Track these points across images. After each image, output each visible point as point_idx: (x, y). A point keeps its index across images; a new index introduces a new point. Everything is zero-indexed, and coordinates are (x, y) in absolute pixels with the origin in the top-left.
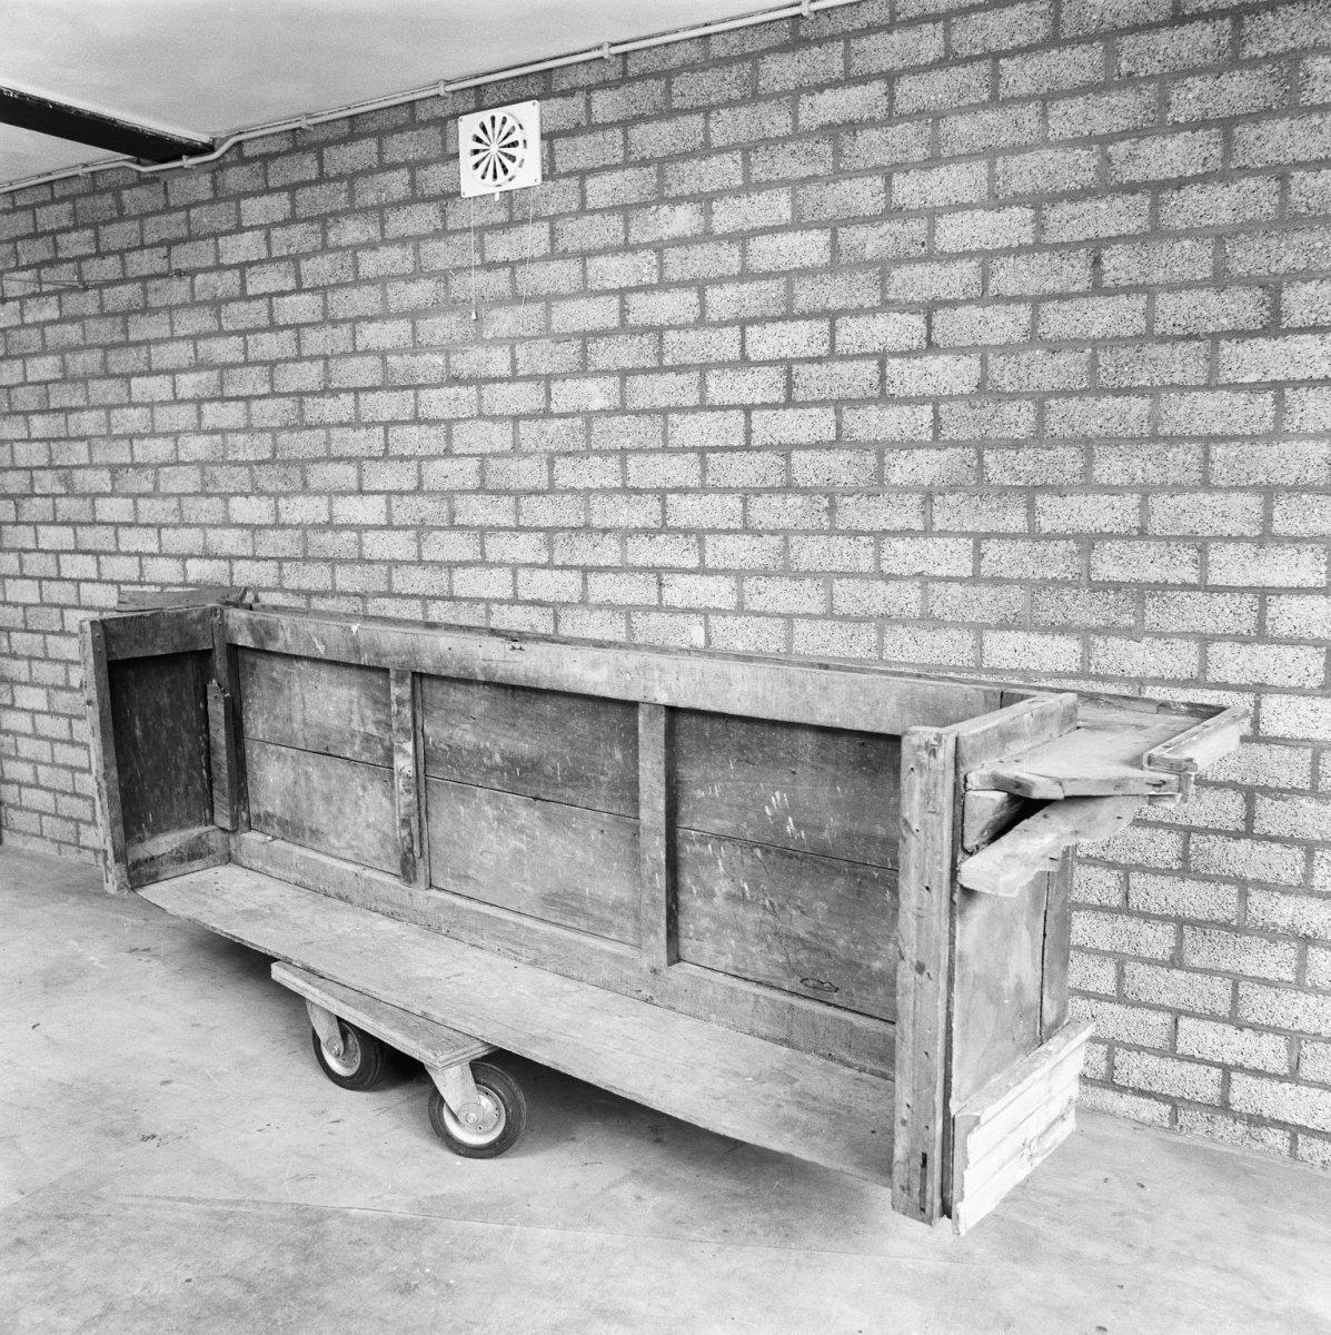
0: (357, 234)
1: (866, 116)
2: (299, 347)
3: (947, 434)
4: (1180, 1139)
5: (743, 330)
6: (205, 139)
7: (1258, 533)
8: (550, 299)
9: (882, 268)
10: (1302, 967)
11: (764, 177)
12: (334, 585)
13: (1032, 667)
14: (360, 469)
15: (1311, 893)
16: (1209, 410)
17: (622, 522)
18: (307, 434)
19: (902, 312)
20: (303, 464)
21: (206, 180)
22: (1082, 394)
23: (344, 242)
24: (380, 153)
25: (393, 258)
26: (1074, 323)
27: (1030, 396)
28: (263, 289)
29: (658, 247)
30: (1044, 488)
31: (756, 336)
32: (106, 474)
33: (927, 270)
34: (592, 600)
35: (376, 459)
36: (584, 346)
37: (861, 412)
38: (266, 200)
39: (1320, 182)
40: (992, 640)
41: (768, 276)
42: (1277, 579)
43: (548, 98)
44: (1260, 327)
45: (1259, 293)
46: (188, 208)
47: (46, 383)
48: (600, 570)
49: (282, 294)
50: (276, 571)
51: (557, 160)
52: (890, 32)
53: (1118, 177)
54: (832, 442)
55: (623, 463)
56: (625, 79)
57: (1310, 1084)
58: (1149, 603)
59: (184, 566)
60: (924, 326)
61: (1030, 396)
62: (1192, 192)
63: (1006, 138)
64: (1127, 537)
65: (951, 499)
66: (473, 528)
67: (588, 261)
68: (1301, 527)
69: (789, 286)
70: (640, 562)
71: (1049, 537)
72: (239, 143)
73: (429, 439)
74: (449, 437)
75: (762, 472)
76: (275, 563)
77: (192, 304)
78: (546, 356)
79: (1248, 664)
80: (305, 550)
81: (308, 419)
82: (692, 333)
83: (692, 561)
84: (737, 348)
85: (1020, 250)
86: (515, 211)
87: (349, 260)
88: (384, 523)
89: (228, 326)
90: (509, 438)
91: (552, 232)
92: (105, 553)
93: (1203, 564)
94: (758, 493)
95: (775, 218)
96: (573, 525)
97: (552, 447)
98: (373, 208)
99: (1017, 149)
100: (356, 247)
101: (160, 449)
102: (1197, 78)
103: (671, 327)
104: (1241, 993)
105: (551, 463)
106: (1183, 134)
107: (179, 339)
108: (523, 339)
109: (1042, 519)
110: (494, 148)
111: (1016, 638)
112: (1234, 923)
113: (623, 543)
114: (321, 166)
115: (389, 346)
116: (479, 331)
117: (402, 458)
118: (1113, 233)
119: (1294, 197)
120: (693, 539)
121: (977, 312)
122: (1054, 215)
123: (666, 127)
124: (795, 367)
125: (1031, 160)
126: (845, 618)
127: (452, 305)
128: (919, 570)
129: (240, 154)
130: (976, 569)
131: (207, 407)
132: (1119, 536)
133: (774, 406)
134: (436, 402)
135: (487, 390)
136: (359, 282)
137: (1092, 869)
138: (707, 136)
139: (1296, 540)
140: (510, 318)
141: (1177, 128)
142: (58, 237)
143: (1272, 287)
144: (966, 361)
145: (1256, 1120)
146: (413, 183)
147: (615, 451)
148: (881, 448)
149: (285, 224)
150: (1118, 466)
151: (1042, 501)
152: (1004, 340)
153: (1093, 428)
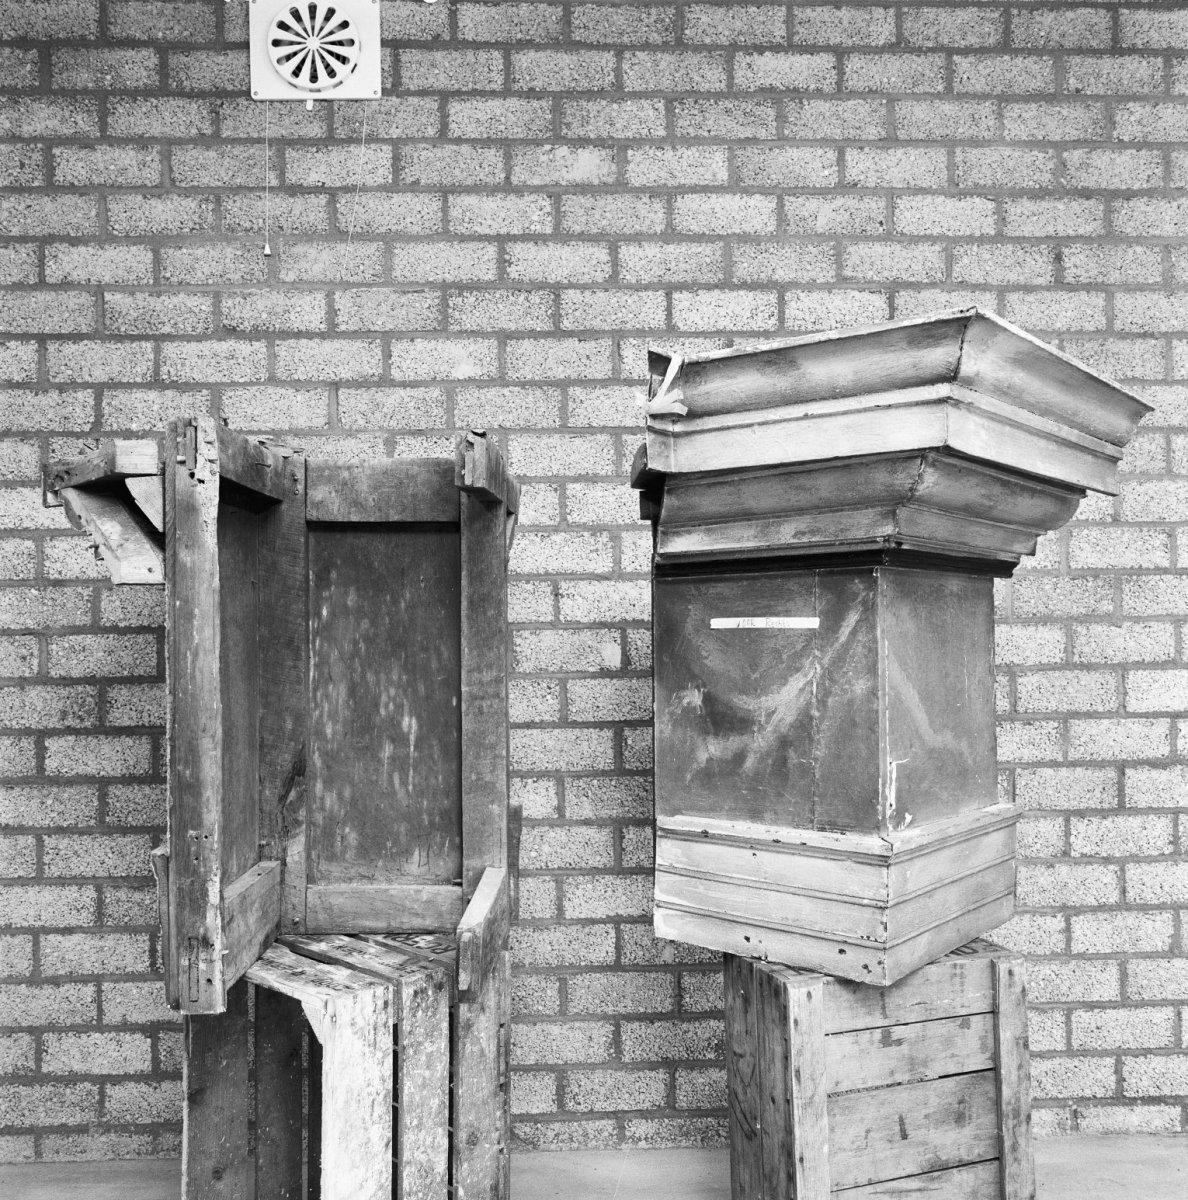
1: (812, 87)
5: (668, 296)
8: (390, 240)
9: (837, 243)
13: (1016, 661)
26: (1040, 315)
29: (555, 193)
31: (686, 304)
51: (405, 74)
58: (1126, 588)
60: (885, 306)
62: (1140, 204)
63: (963, 131)
64: (1101, 524)
67: (451, 198)
69: (727, 254)
78: (384, 308)
82: (601, 294)
84: (661, 316)
85: (982, 240)
87: (37, 157)
91: (396, 158)
95: (708, 176)
97: (393, 423)
98: (85, 91)
99: (975, 142)
102: (1137, 104)
103: (571, 286)
106: (1129, 152)
108: (346, 285)
115: (107, 279)
118: (1071, 233)
120: (604, 537)
123: (565, 59)
125: (991, 155)
127: (227, 234)
134: (191, 360)
135: (283, 348)
137: (1089, 868)
141: (1122, 145)
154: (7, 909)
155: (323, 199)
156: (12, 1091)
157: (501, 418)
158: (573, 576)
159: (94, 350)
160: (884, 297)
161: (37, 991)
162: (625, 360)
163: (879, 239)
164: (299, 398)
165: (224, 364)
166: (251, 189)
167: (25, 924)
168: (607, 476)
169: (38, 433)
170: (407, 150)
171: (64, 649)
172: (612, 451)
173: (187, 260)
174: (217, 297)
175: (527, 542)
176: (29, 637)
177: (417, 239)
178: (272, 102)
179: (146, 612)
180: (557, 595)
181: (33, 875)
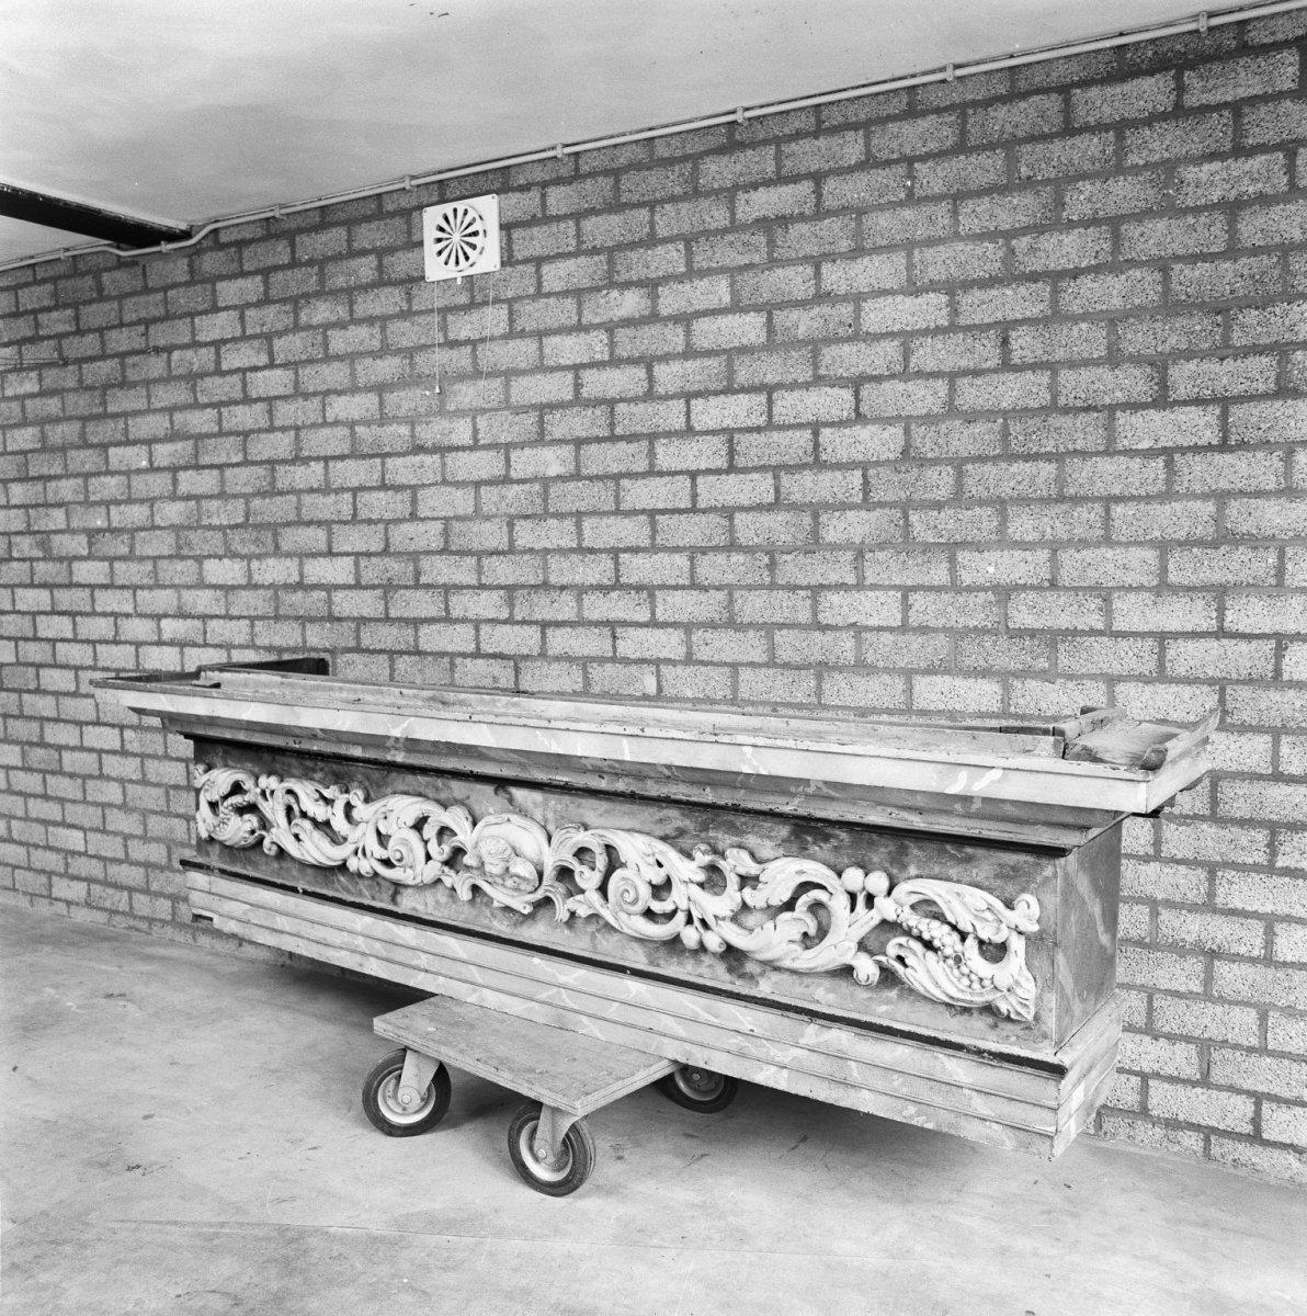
0: (327, 314)
2: (271, 419)
3: (875, 497)
4: (1103, 1144)
5: (688, 402)
6: (183, 226)
7: (1155, 583)
8: (510, 374)
9: (814, 346)
10: (1208, 980)
11: (705, 265)
12: (305, 642)
14: (330, 533)
15: (1215, 910)
16: (1107, 474)
17: (578, 579)
18: (278, 500)
19: (833, 386)
20: (275, 528)
21: (183, 264)
22: (995, 459)
23: (314, 321)
24: (349, 241)
25: (362, 336)
27: (950, 461)
28: (237, 364)
29: (610, 328)
30: (963, 545)
31: (700, 408)
32: (83, 539)
33: (855, 349)
34: (550, 653)
35: (345, 523)
36: (541, 418)
37: (797, 476)
38: (240, 282)
39: (1197, 273)
40: (921, 684)
41: (709, 353)
42: (1174, 625)
43: (506, 192)
44: (1150, 399)
45: (1148, 370)
46: (165, 289)
47: (24, 453)
48: (559, 624)
49: (255, 369)
50: (248, 630)
51: (515, 247)
52: (816, 138)
53: (1022, 267)
54: (770, 504)
55: (579, 525)
56: (577, 176)
57: (1219, 1088)
59: (159, 625)
60: (852, 399)
61: (950, 461)
62: (1086, 282)
63: (921, 232)
64: (1038, 588)
65: (880, 555)
66: (437, 587)
67: (544, 339)
68: (1193, 578)
71: (970, 589)
72: (215, 231)
73: (397, 504)
74: (414, 501)
76: (247, 622)
77: (168, 379)
79: (1150, 702)
80: (277, 609)
81: (279, 485)
83: (643, 615)
84: (683, 419)
85: (937, 331)
86: (475, 293)
87: (320, 337)
89: (203, 399)
90: (471, 503)
91: (511, 313)
92: (82, 614)
93: (1107, 611)
94: (704, 551)
98: (342, 290)
99: (931, 242)
100: (326, 326)
101: (137, 514)
102: (1087, 182)
103: (622, 400)
104: (1155, 1005)
105: (511, 525)
106: (1076, 231)
107: (155, 411)
108: (484, 411)
109: (963, 572)
110: (456, 237)
111: (943, 682)
112: (1147, 940)
113: (579, 600)
114: (293, 252)
115: (357, 417)
116: (442, 404)
117: (370, 522)
118: (1019, 316)
119: (1175, 286)
120: (644, 594)
121: (901, 386)
122: (967, 300)
124: (736, 436)
125: (944, 252)
126: (786, 666)
128: (853, 620)
129: (216, 240)
130: (905, 618)
131: (182, 475)
132: (1033, 588)
133: (717, 472)
134: (402, 470)
135: (450, 458)
136: (328, 358)
138: (652, 227)
139: (1190, 589)
140: (471, 391)
141: (1071, 225)
142: (40, 316)
143: (1159, 365)
144: (891, 430)
145: (1173, 1124)
146: (380, 268)
147: (571, 514)
148: (816, 510)
149: (259, 304)
150: (1029, 525)
151: (963, 556)
152: (924, 411)
153: (1006, 490)
155: (469, 349)
158: (625, 624)
159: (350, 464)
160: (851, 391)
163: (848, 339)
166: (429, 346)
170: (516, 306)
173: (397, 400)
174: (413, 424)
177: (523, 373)
178: (438, 282)
180: (614, 637)
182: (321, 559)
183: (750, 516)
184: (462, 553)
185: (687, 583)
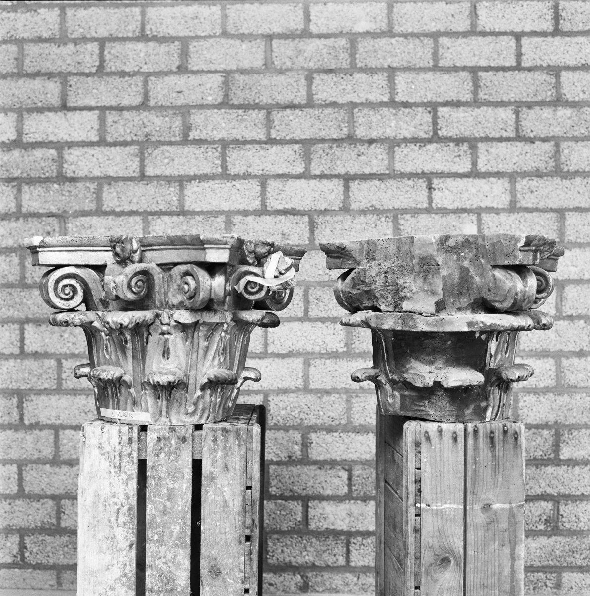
12: (19, 206)
14: (65, 84)
17: (390, 132)
34: (354, 206)
35: (88, 75)
48: (364, 177)
55: (391, 80)
70: (408, 169)
74: (184, 54)
75: (533, 88)
88: (95, 138)
94: (530, 106)
96: (335, 136)
97: (312, 64)
105: (310, 80)
113: (391, 153)
117: (122, 74)
120: (465, 147)
133: (544, 34)
154: (36, 411)
156: (41, 538)
157: (390, 60)
158: (442, 175)
161: (57, 470)
162: (480, 18)
164: (244, 46)
165: (190, 23)
167: (49, 422)
168: (467, 102)
169: (60, 74)
171: (77, 226)
172: (471, 84)
175: (409, 150)
176: (51, 219)
179: (135, 200)
180: (430, 188)
181: (54, 387)
182: (51, 114)
183: (577, 74)
184: (246, 107)
185: (512, 135)
